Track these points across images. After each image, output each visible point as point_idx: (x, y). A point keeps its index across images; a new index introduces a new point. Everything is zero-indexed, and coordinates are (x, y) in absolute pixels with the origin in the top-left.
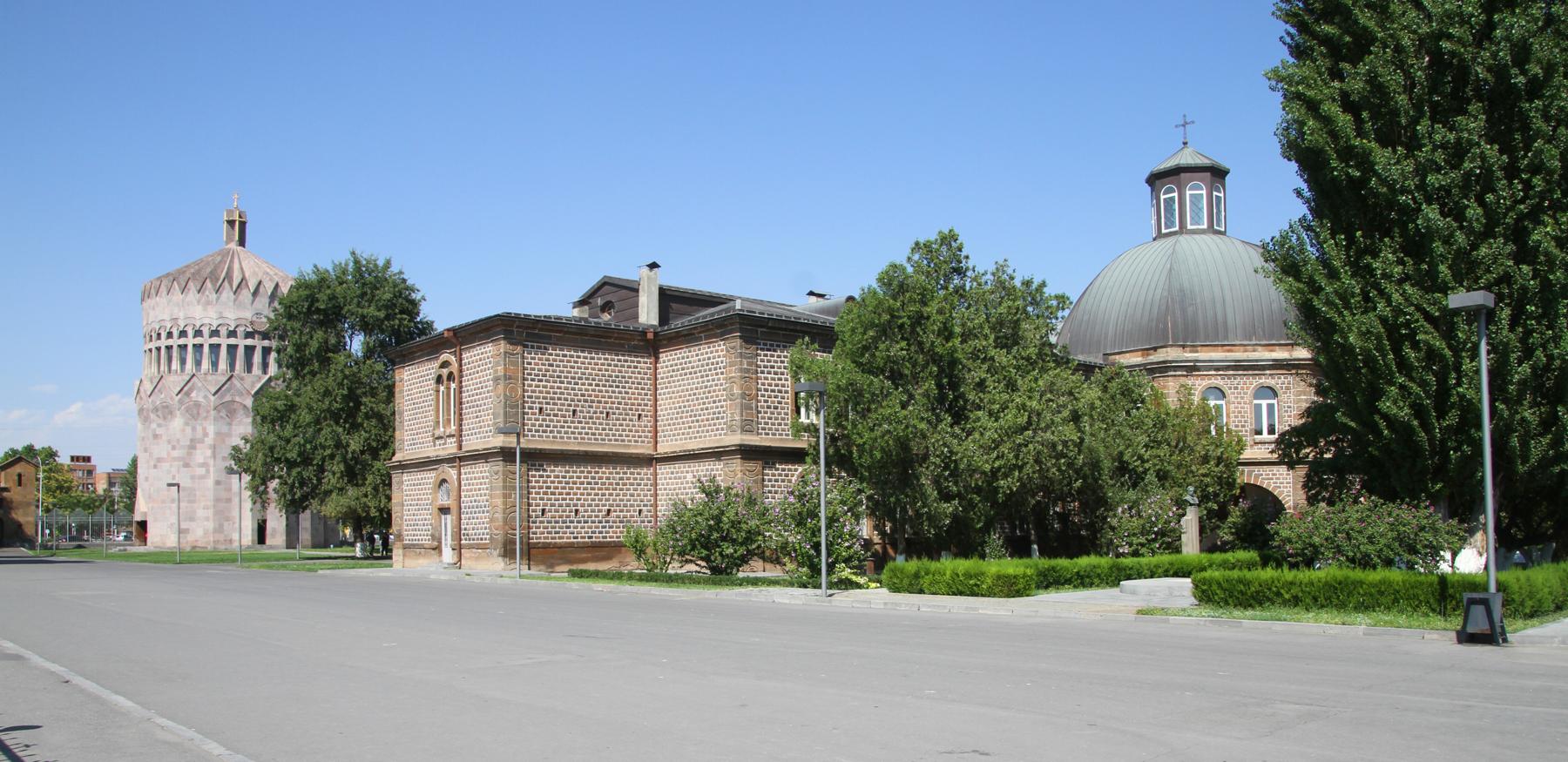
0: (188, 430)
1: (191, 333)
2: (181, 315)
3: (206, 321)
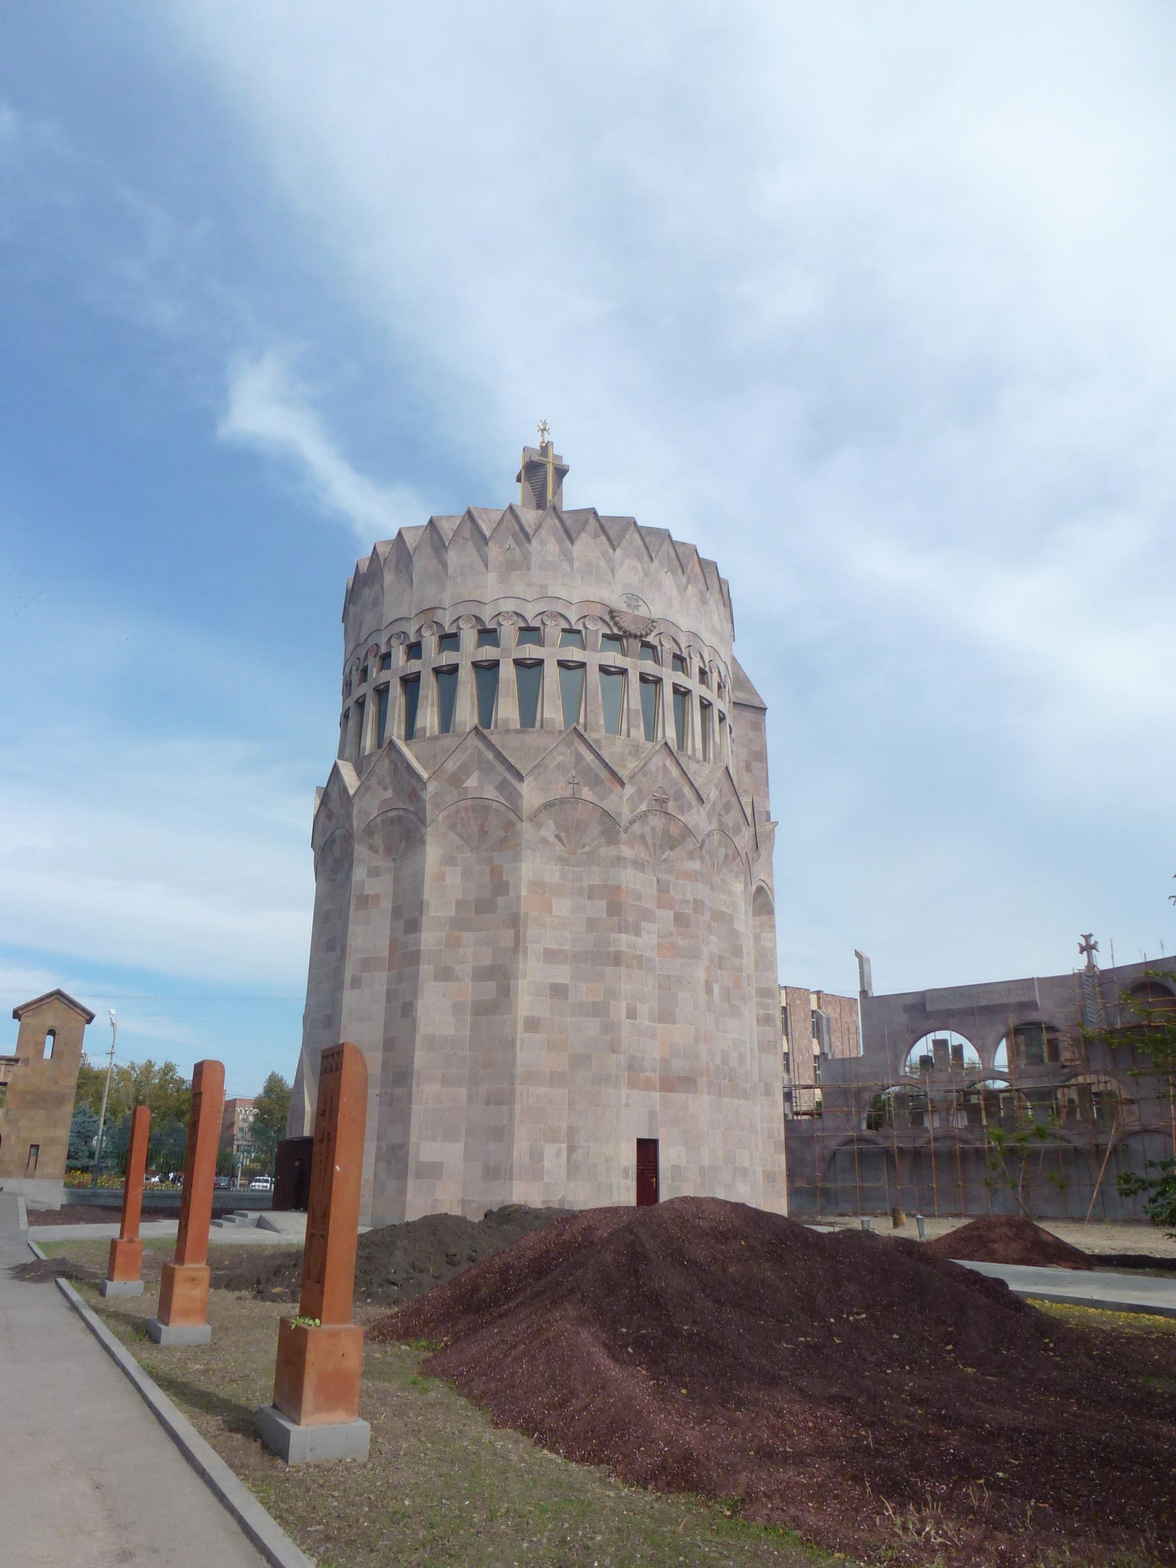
0: (454, 877)
1: (469, 637)
2: (447, 599)
3: (509, 606)
